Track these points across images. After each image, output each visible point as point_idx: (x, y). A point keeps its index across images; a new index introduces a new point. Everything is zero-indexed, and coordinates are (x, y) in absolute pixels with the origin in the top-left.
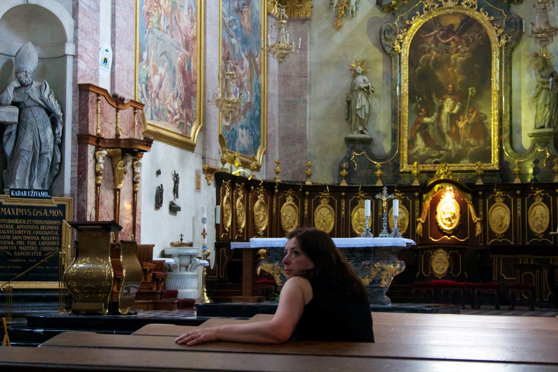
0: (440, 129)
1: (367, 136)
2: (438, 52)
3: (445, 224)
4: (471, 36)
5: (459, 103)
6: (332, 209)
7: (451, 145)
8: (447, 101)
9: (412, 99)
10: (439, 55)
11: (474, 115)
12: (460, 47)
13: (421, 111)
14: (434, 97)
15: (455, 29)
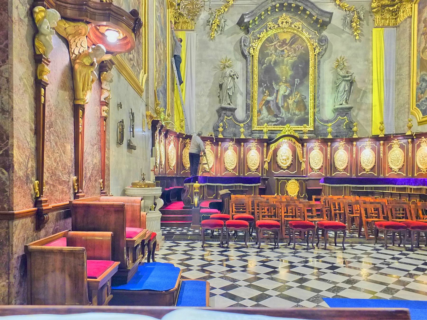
0: (277, 104)
1: (232, 106)
2: (276, 56)
3: (282, 163)
4: (297, 47)
5: (289, 88)
6: (212, 152)
7: (284, 114)
8: (281, 87)
9: (260, 85)
10: (277, 58)
11: (298, 96)
12: (290, 53)
13: (265, 93)
14: (274, 83)
15: (287, 42)
